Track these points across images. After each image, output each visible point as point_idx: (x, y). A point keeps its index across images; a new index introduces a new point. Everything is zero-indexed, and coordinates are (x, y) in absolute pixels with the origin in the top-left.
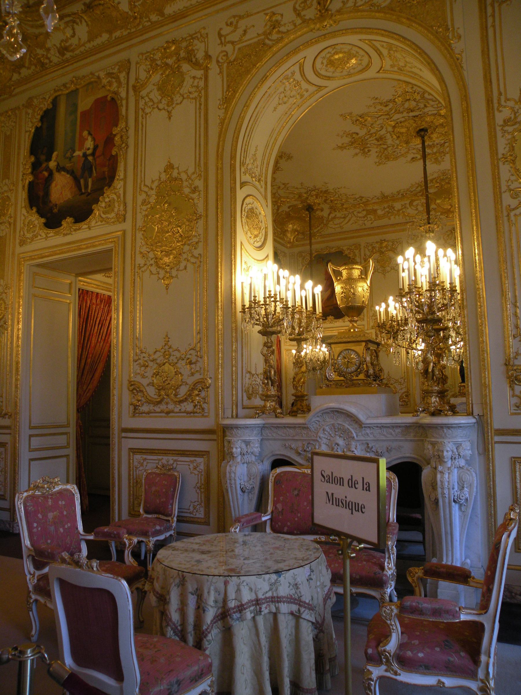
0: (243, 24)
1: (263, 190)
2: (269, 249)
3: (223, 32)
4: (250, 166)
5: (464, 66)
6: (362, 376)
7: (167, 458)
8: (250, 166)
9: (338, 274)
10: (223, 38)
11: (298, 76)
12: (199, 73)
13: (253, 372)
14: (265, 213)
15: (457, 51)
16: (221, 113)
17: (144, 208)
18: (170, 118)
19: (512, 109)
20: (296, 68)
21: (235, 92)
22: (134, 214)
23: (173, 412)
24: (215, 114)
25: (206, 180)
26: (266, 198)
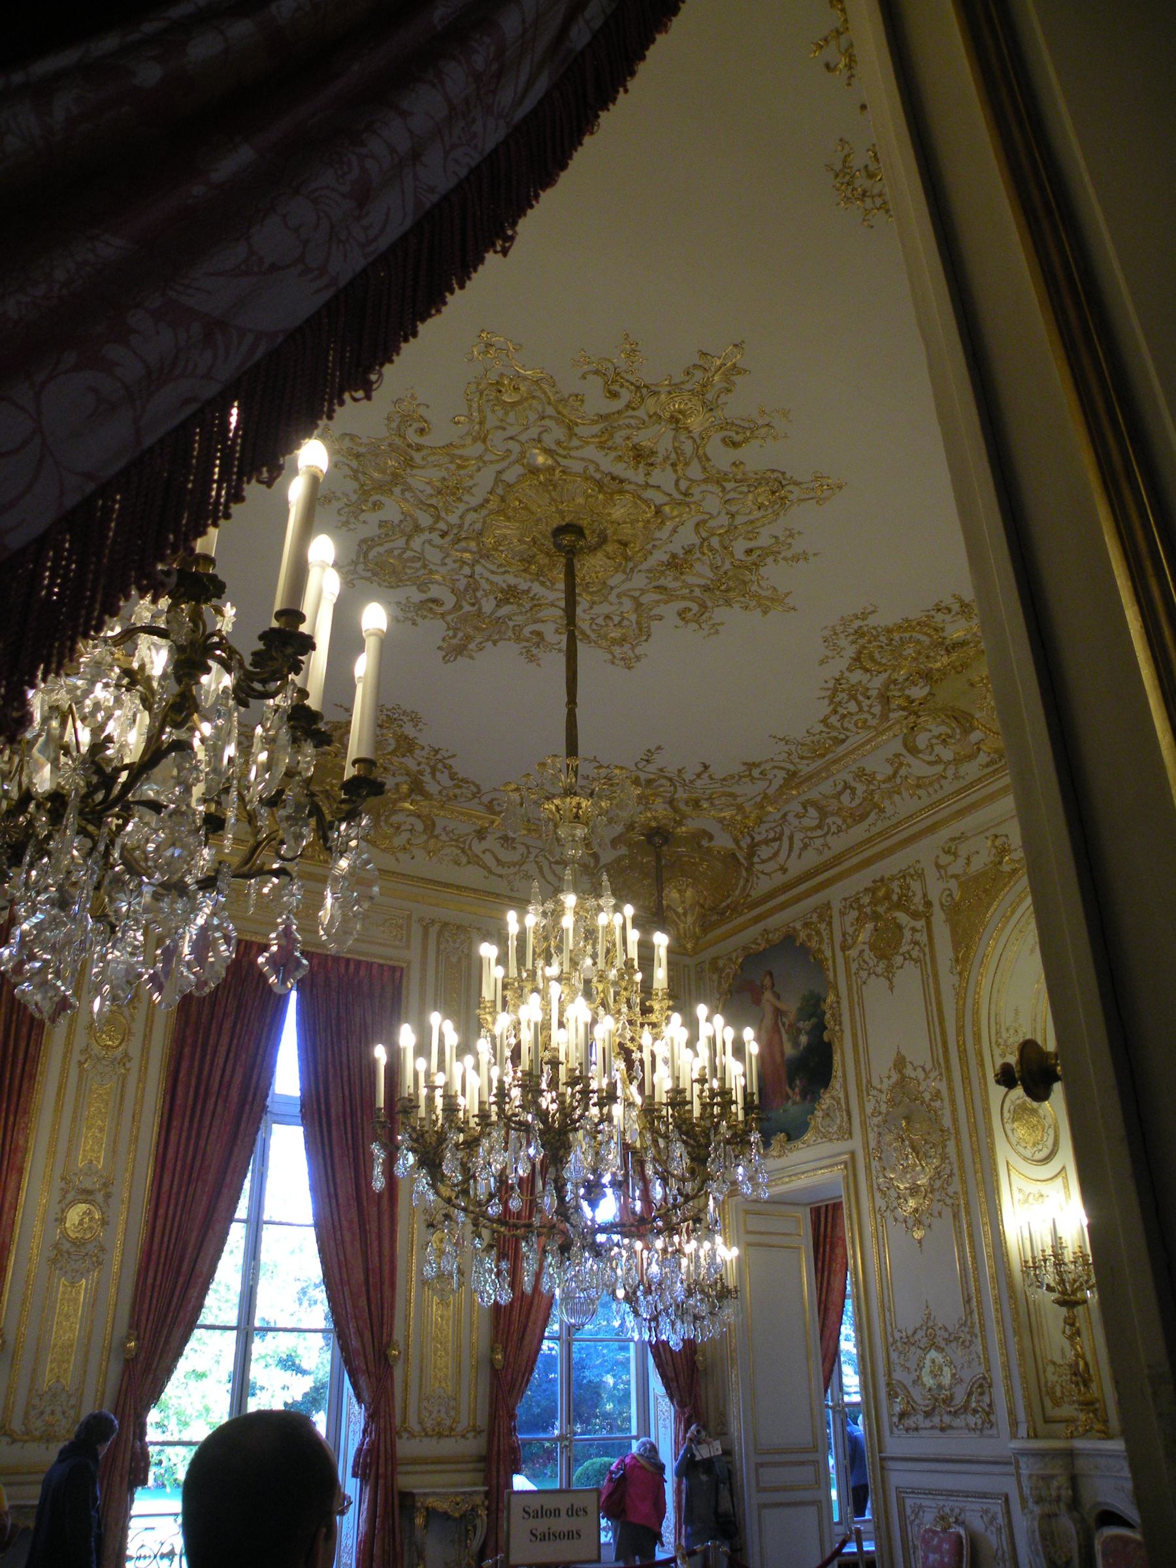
3: (941, 863)
7: (951, 1504)
10: (943, 872)
12: (920, 924)
13: (1060, 1361)
16: (955, 979)
17: (875, 1120)
18: (891, 988)
21: (968, 947)
22: (863, 1124)
23: (951, 1427)
24: (948, 981)
25: (950, 1081)
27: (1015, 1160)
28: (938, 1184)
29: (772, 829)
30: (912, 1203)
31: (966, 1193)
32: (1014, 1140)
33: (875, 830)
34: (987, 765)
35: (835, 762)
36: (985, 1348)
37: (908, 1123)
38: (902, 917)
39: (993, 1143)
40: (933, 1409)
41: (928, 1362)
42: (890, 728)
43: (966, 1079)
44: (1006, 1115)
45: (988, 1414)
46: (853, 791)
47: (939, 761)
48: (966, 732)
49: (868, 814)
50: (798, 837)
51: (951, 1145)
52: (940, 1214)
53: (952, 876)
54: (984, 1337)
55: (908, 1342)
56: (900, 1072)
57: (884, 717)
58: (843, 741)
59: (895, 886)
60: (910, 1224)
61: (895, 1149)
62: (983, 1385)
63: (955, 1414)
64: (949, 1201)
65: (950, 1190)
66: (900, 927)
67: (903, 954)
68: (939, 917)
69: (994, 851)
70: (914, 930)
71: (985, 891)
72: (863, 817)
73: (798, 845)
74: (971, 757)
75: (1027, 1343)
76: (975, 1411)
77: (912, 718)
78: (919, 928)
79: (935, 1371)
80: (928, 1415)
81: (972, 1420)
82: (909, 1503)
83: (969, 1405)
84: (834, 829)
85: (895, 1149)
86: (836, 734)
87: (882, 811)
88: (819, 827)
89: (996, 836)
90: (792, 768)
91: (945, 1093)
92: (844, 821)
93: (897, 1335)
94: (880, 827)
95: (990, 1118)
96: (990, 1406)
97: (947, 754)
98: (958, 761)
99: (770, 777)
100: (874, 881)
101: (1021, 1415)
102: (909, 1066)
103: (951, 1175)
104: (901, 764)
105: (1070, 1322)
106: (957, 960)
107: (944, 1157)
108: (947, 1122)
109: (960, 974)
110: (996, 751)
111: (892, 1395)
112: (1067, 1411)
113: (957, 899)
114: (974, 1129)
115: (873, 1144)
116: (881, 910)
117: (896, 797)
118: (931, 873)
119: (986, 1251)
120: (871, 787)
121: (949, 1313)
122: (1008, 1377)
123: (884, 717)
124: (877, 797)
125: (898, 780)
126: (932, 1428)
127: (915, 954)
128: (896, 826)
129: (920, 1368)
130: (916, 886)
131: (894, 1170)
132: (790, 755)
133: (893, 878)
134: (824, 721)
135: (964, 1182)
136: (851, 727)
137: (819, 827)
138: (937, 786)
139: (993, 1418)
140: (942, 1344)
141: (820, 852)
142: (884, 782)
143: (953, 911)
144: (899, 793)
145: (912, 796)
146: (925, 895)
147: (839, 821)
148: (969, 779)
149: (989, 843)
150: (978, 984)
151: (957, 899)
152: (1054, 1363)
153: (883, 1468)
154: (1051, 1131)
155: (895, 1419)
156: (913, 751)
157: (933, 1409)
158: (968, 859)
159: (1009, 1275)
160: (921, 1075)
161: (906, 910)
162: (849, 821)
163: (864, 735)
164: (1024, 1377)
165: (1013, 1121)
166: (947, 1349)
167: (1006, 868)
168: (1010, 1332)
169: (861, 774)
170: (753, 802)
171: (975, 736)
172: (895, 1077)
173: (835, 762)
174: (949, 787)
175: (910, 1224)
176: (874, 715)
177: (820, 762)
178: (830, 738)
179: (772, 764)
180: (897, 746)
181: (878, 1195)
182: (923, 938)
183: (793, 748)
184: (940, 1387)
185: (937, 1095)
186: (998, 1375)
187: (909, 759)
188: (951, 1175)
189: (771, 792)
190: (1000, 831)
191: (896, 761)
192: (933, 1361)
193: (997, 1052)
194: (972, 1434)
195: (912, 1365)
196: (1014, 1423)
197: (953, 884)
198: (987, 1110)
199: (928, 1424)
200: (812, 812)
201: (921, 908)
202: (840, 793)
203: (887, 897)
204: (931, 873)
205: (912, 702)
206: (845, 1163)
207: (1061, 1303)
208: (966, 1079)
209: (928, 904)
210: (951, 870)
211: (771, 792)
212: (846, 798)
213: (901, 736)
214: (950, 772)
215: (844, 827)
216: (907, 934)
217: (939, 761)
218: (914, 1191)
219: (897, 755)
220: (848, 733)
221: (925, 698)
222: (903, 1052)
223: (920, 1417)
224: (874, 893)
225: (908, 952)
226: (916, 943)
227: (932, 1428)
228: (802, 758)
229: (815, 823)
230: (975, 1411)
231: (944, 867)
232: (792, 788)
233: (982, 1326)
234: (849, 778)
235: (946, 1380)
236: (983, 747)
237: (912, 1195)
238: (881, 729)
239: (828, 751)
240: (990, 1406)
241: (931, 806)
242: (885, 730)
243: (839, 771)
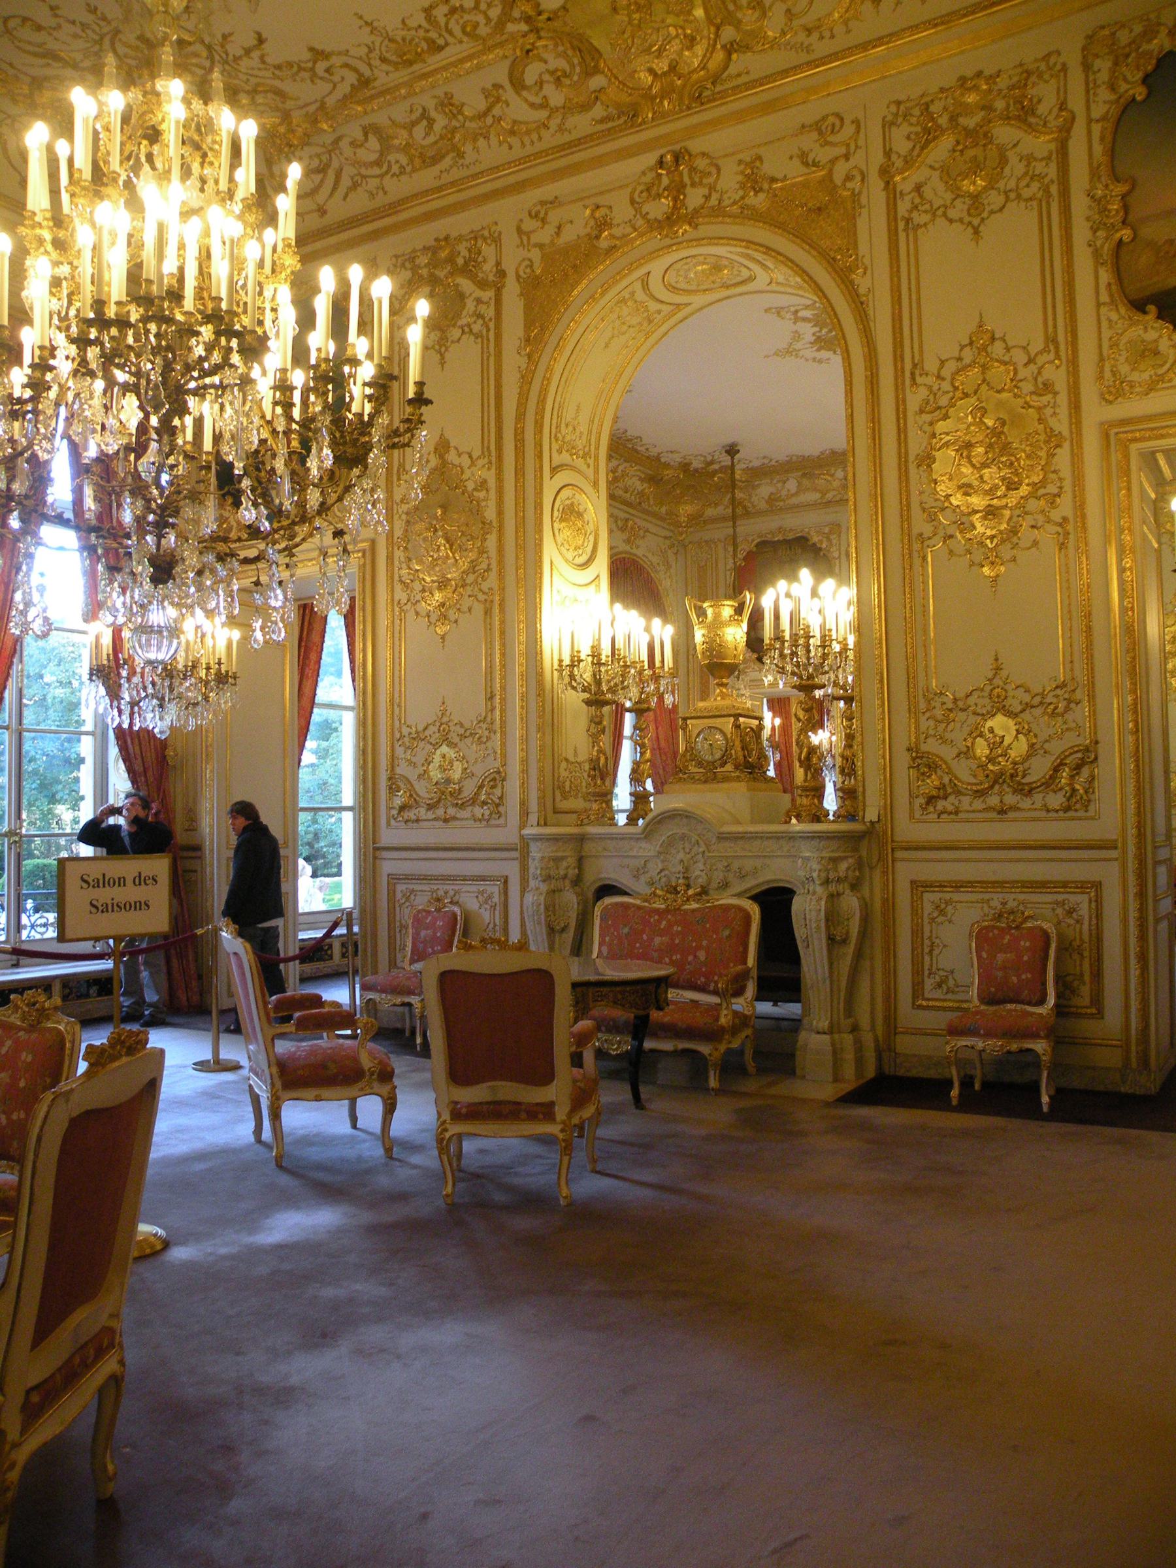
0: (554, 216)
1: (590, 472)
2: (601, 566)
3: (525, 227)
4: (568, 438)
5: (871, 312)
6: (729, 767)
8: (568, 438)
9: (701, 613)
10: (525, 238)
11: (640, 295)
12: (488, 294)
13: (572, 759)
14: (595, 509)
15: (862, 291)
16: (523, 362)
18: (442, 363)
19: (930, 388)
20: (638, 286)
21: (543, 329)
23: (454, 818)
24: (513, 362)
26: (595, 484)
27: (559, 562)
28: (471, 578)
29: (318, 155)
30: (438, 596)
31: (503, 589)
32: (559, 539)
33: (446, 178)
34: (602, 121)
35: (425, 76)
36: (503, 744)
37: (444, 513)
38: (466, 285)
39: (541, 540)
40: (439, 801)
41: (437, 758)
42: (501, 45)
43: (519, 472)
44: (556, 514)
45: (498, 805)
46: (431, 122)
47: (544, 105)
48: (589, 73)
49: (443, 157)
50: (349, 171)
51: (492, 541)
52: (470, 609)
53: (536, 245)
54: (503, 734)
55: (418, 737)
56: (441, 457)
57: (500, 25)
58: (441, 48)
59: (463, 248)
60: (433, 619)
61: (425, 539)
62: (497, 778)
63: (462, 806)
64: (481, 597)
65: (485, 586)
66: (462, 296)
67: (462, 327)
68: (512, 288)
69: (592, 222)
70: (479, 301)
71: (575, 267)
72: (436, 159)
73: (346, 182)
74: (585, 107)
75: (548, 738)
76: (484, 803)
77: (532, 38)
78: (485, 299)
79: (445, 763)
80: (430, 807)
81: (478, 811)
82: (400, 888)
83: (487, 796)
84: (395, 168)
85: (425, 539)
86: (433, 35)
87: (461, 155)
88: (378, 163)
89: (598, 207)
90: (367, 72)
91: (492, 483)
92: (411, 161)
93: (405, 731)
94: (456, 174)
95: (541, 514)
96: (501, 798)
97: (556, 98)
98: (568, 109)
99: (336, 78)
100: (436, 240)
101: (533, 806)
102: (453, 452)
103: (488, 570)
104: (498, 100)
105: (596, 721)
106: (528, 340)
107: (482, 551)
108: (490, 514)
109: (529, 356)
110: (618, 105)
111: (393, 789)
112: (577, 803)
113: (538, 272)
114: (521, 523)
115: (398, 533)
116: (441, 274)
117: (481, 142)
118: (510, 240)
119: (519, 647)
120: (455, 123)
121: (468, 707)
122: (525, 771)
123: (500, 25)
124: (458, 136)
125: (489, 120)
126: (435, 819)
127: (476, 328)
128: (474, 176)
129: (429, 762)
130: (488, 251)
131: (420, 562)
132: (371, 50)
133: (460, 239)
134: (428, 11)
135: (501, 576)
136: (457, 30)
137: (378, 163)
138: (535, 136)
139: (501, 809)
140: (456, 740)
141: (372, 195)
142: (472, 119)
143: (531, 286)
144: (487, 137)
145: (500, 143)
146: (498, 264)
147: (404, 160)
148: (575, 135)
149: (588, 212)
150: (549, 369)
151: (538, 272)
152: (567, 760)
153: (375, 858)
154: (592, 538)
155: (395, 812)
156: (518, 84)
157: (439, 801)
158: (559, 227)
159: (540, 674)
160: (466, 461)
161: (473, 277)
162: (417, 161)
163: (468, 47)
164: (541, 770)
165: (562, 520)
166: (461, 745)
167: (604, 243)
168: (533, 729)
169: (448, 104)
170: (303, 112)
171: (597, 82)
172: (434, 461)
173: (425, 76)
174: (550, 139)
175: (433, 619)
176: (489, 20)
177: (403, 75)
178: (426, 39)
179: (344, 59)
180: (500, 74)
181: (398, 587)
182: (490, 312)
183: (379, 40)
184: (448, 781)
185: (483, 485)
186: (514, 768)
187: (509, 94)
188: (488, 570)
189: (331, 101)
190: (600, 200)
191: (493, 95)
192: (444, 756)
193: (555, 446)
194: (478, 824)
195: (420, 758)
196: (525, 813)
197: (535, 255)
198: (539, 506)
199: (430, 815)
200: (373, 143)
201: (491, 278)
202: (414, 124)
203: (451, 260)
204: (510, 240)
205: (540, 14)
206: (364, 552)
207: (588, 703)
208: (519, 472)
209: (502, 274)
210: (535, 239)
211: (331, 101)
212: (419, 131)
213: (507, 63)
214: (553, 124)
215: (408, 169)
216: (470, 305)
217: (544, 105)
218: (443, 584)
219: (497, 86)
220: (450, 40)
221: (555, 13)
222: (447, 435)
223: (423, 811)
224: (434, 253)
225: (469, 325)
226: (480, 316)
227: (435, 819)
228: (383, 60)
229: (374, 157)
230: (484, 803)
231: (528, 234)
232: (358, 103)
233: (503, 723)
234: (431, 104)
235: (456, 775)
236: (603, 97)
237: (439, 588)
238: (490, 43)
239: (419, 57)
240: (501, 798)
241: (520, 161)
242: (495, 46)
243: (422, 91)
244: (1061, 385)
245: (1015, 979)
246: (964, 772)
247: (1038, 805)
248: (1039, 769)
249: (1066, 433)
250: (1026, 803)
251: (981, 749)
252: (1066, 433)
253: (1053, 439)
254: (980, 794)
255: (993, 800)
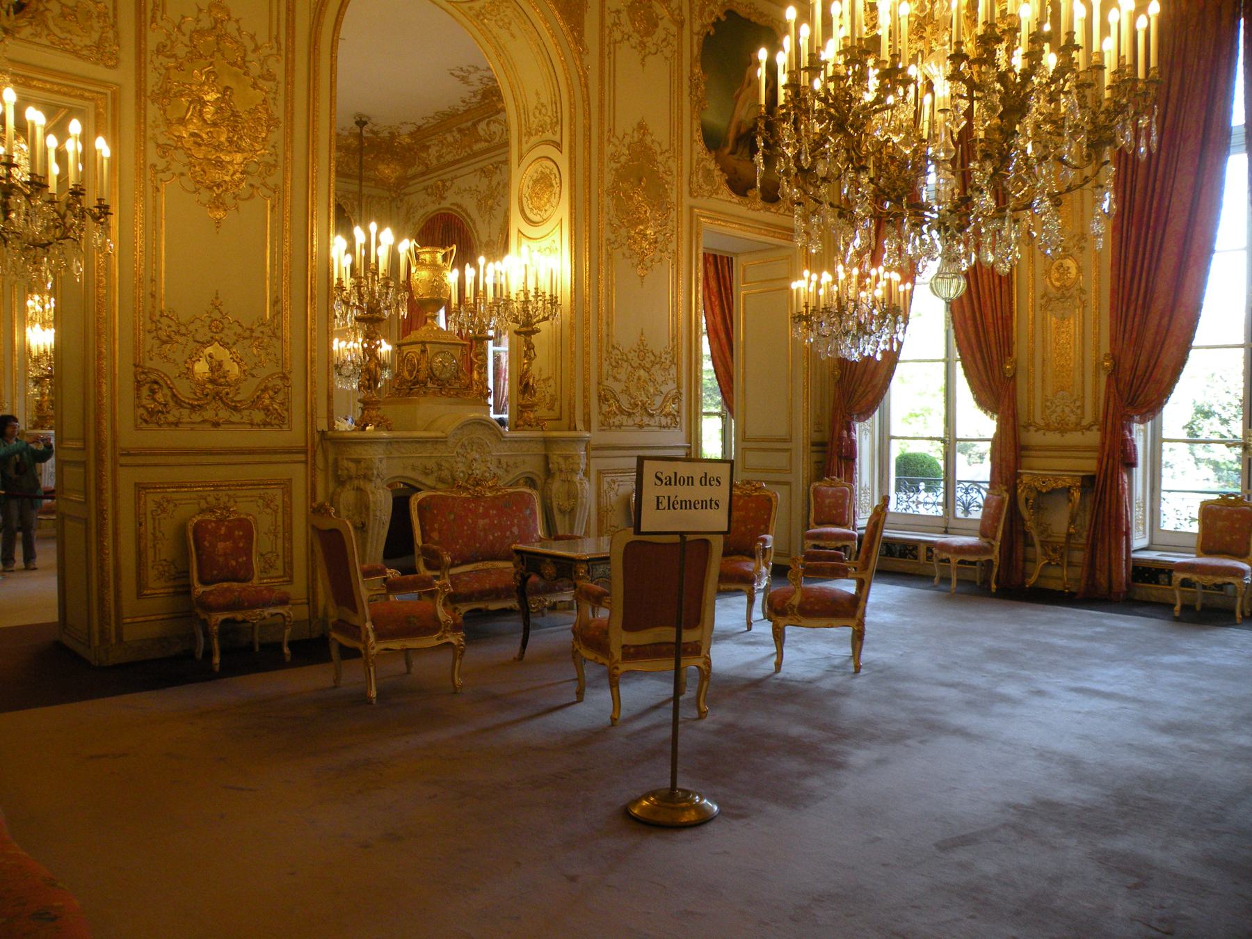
244: (281, 76)
245: (234, 563)
246: (184, 390)
247: (246, 420)
248: (246, 393)
249: (282, 119)
250: (236, 417)
251: (201, 368)
252: (282, 119)
253: (272, 122)
254: (193, 408)
255: (209, 414)
